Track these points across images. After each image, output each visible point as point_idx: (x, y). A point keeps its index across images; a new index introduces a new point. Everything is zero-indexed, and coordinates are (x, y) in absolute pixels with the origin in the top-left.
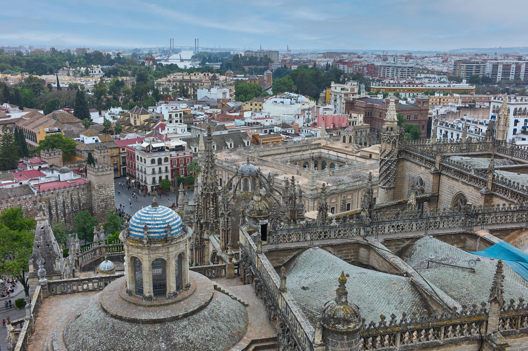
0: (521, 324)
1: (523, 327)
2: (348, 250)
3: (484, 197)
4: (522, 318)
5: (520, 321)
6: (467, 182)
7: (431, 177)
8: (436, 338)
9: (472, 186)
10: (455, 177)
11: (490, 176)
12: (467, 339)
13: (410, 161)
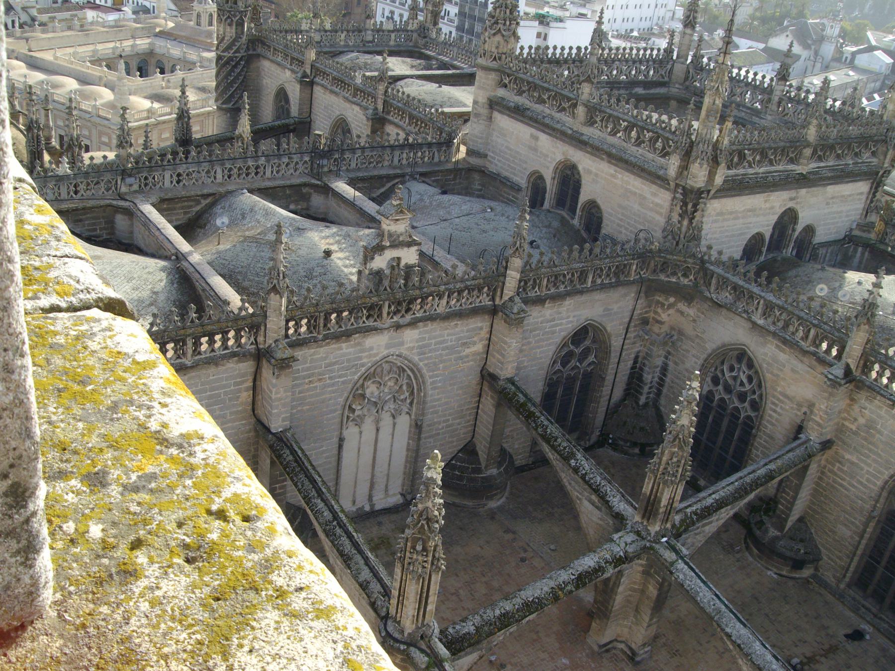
0: (325, 325)
1: (329, 329)
2: (93, 218)
3: (370, 123)
4: (325, 315)
5: (322, 321)
6: (350, 98)
7: (298, 87)
8: (179, 357)
9: (357, 105)
10: (334, 88)
11: (381, 88)
12: (234, 355)
13: (269, 59)
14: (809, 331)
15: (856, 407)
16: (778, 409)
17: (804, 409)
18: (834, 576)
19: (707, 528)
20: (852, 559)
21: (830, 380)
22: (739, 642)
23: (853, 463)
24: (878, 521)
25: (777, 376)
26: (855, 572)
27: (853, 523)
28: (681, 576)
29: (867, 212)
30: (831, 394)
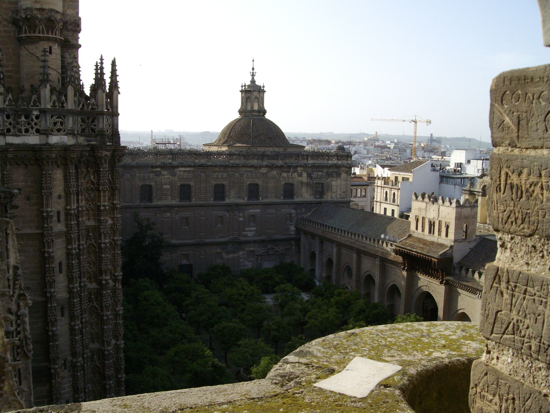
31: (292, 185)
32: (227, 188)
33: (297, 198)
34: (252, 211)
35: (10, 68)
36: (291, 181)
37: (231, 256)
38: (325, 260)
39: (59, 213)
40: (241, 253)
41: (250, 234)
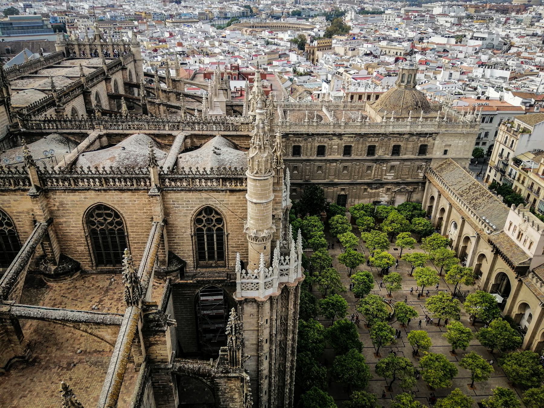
14: (10, 181)
15: (51, 200)
16: (20, 220)
17: (31, 213)
18: (89, 267)
19: (18, 286)
20: (91, 256)
21: (32, 196)
22: (61, 318)
23: (65, 222)
24: (90, 237)
25: (9, 207)
26: (95, 260)
27: (82, 243)
28: (17, 312)
29: (11, 118)
30: (37, 201)
31: (426, 146)
32: (377, 148)
33: (429, 154)
34: (392, 163)
35: (243, 240)
36: (426, 143)
37: (374, 191)
38: (440, 207)
39: (267, 320)
40: (382, 189)
41: (390, 178)
